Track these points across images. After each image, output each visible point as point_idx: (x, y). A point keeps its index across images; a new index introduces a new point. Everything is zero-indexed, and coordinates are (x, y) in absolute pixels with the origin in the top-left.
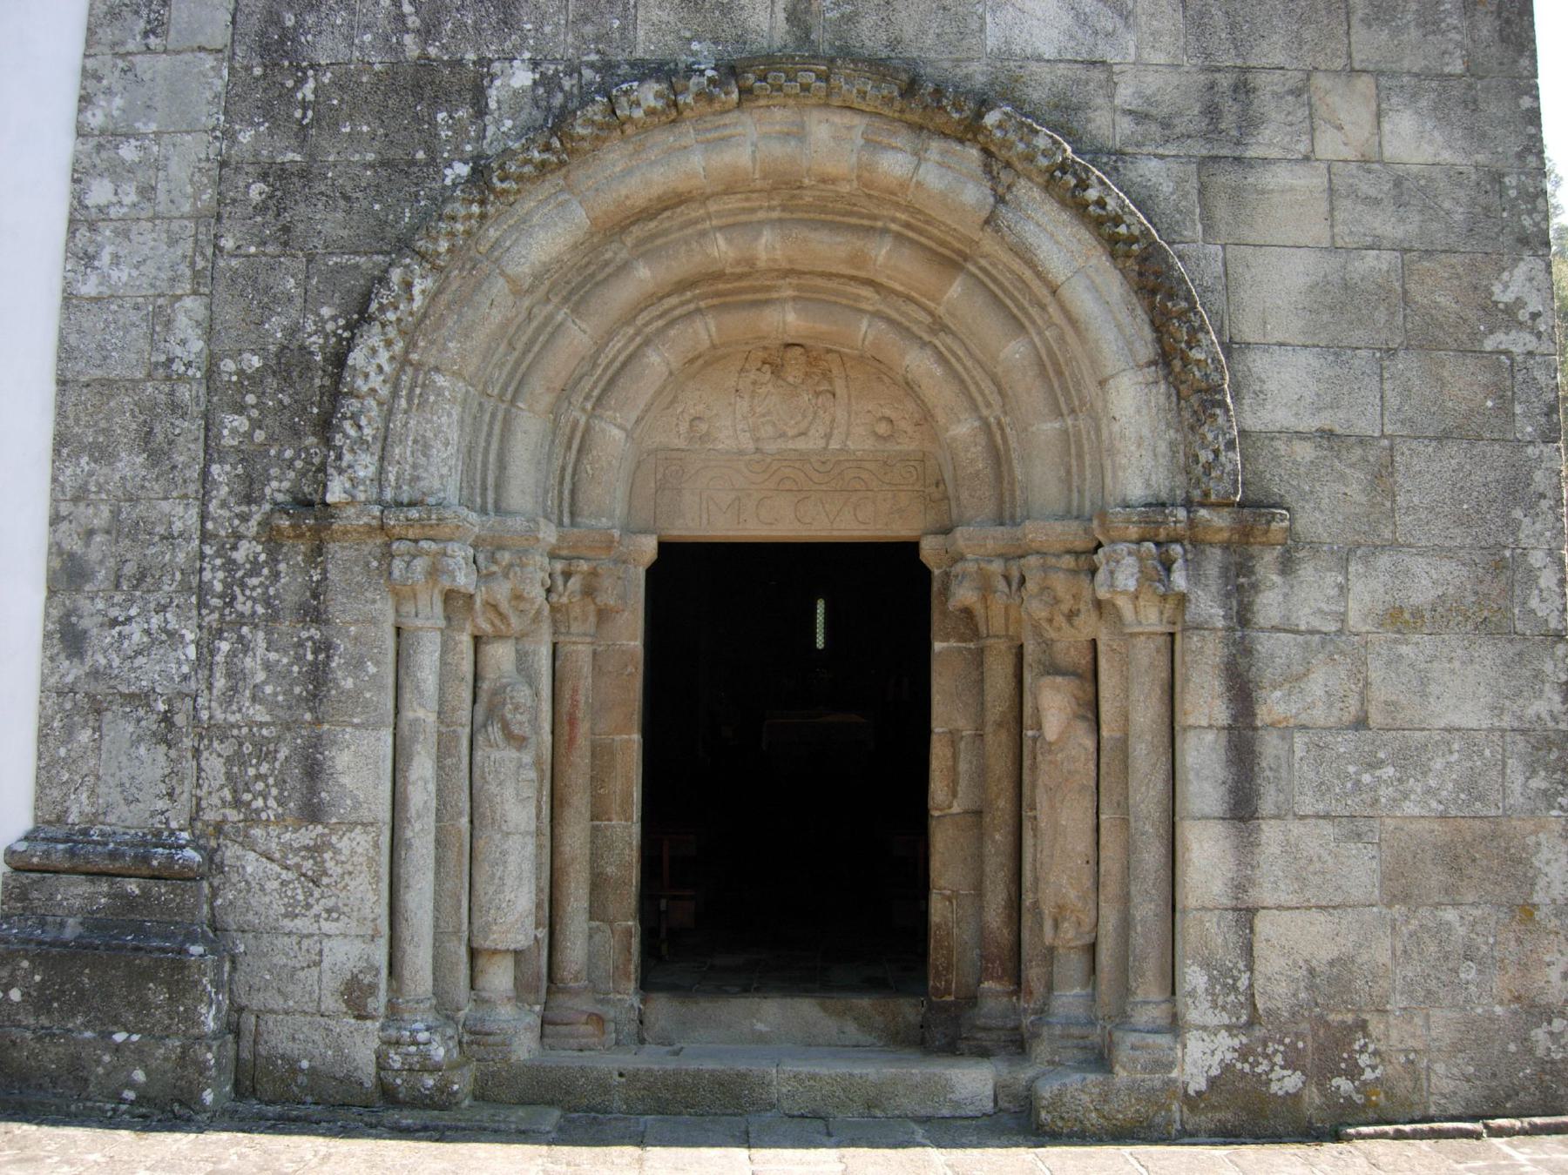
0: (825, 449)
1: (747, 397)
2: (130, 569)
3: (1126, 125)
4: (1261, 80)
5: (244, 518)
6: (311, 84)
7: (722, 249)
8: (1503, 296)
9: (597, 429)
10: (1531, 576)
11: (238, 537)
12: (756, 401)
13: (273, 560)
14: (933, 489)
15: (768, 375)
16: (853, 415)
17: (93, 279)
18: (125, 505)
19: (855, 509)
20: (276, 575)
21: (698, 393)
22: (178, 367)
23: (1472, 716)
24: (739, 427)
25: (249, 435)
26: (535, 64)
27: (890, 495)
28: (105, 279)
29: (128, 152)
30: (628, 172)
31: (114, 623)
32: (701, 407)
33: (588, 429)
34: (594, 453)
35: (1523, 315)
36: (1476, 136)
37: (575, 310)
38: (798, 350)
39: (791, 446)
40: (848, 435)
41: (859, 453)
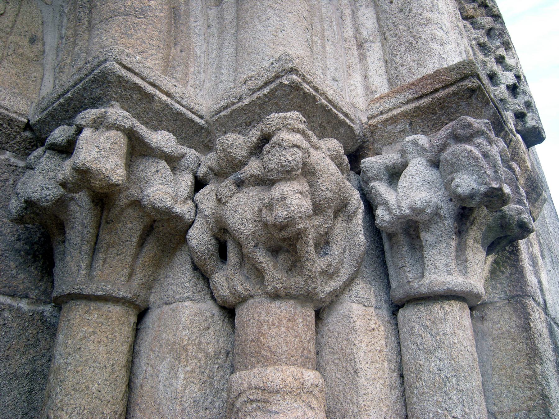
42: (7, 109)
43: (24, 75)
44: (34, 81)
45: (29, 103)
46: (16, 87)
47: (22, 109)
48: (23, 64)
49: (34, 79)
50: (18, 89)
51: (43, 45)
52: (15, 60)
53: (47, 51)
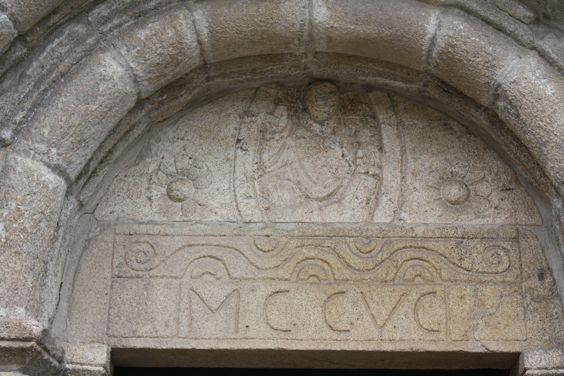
0: (370, 221)
1: (251, 149)
9: (19, 169)
12: (265, 156)
14: (535, 282)
15: (283, 122)
16: (409, 177)
19: (415, 311)
21: (180, 143)
24: (240, 192)
27: (469, 291)
32: (185, 163)
34: (13, 205)
38: (330, 87)
39: (316, 218)
40: (401, 204)
41: (420, 231)
42: (546, 368)
43: (547, 317)
44: (557, 318)
45: (560, 353)
46: (545, 333)
47: (557, 362)
48: (542, 306)
49: (556, 316)
50: (547, 335)
51: (551, 274)
52: (535, 306)
53: (556, 278)
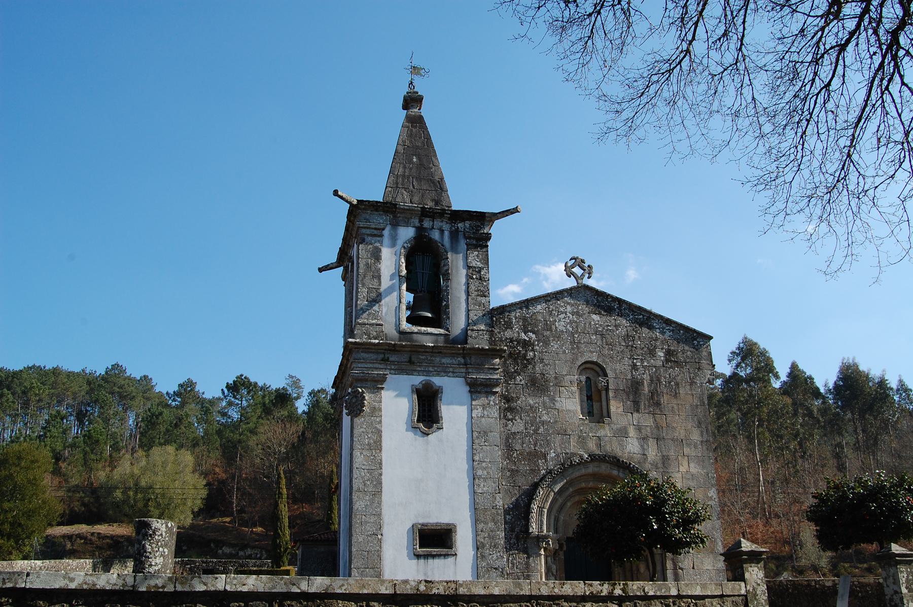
2: (493, 544)
3: (650, 466)
4: (670, 457)
5: (512, 535)
6: (515, 454)
7: (583, 485)
8: (710, 495)
10: (717, 544)
11: (511, 538)
13: (518, 543)
17: (480, 489)
18: (491, 533)
20: (518, 546)
22: (498, 507)
23: (710, 568)
25: (511, 519)
26: (555, 453)
28: (482, 490)
29: (484, 464)
30: (572, 473)
31: (491, 554)
33: (558, 517)
35: (713, 498)
36: (703, 468)
37: (560, 496)
